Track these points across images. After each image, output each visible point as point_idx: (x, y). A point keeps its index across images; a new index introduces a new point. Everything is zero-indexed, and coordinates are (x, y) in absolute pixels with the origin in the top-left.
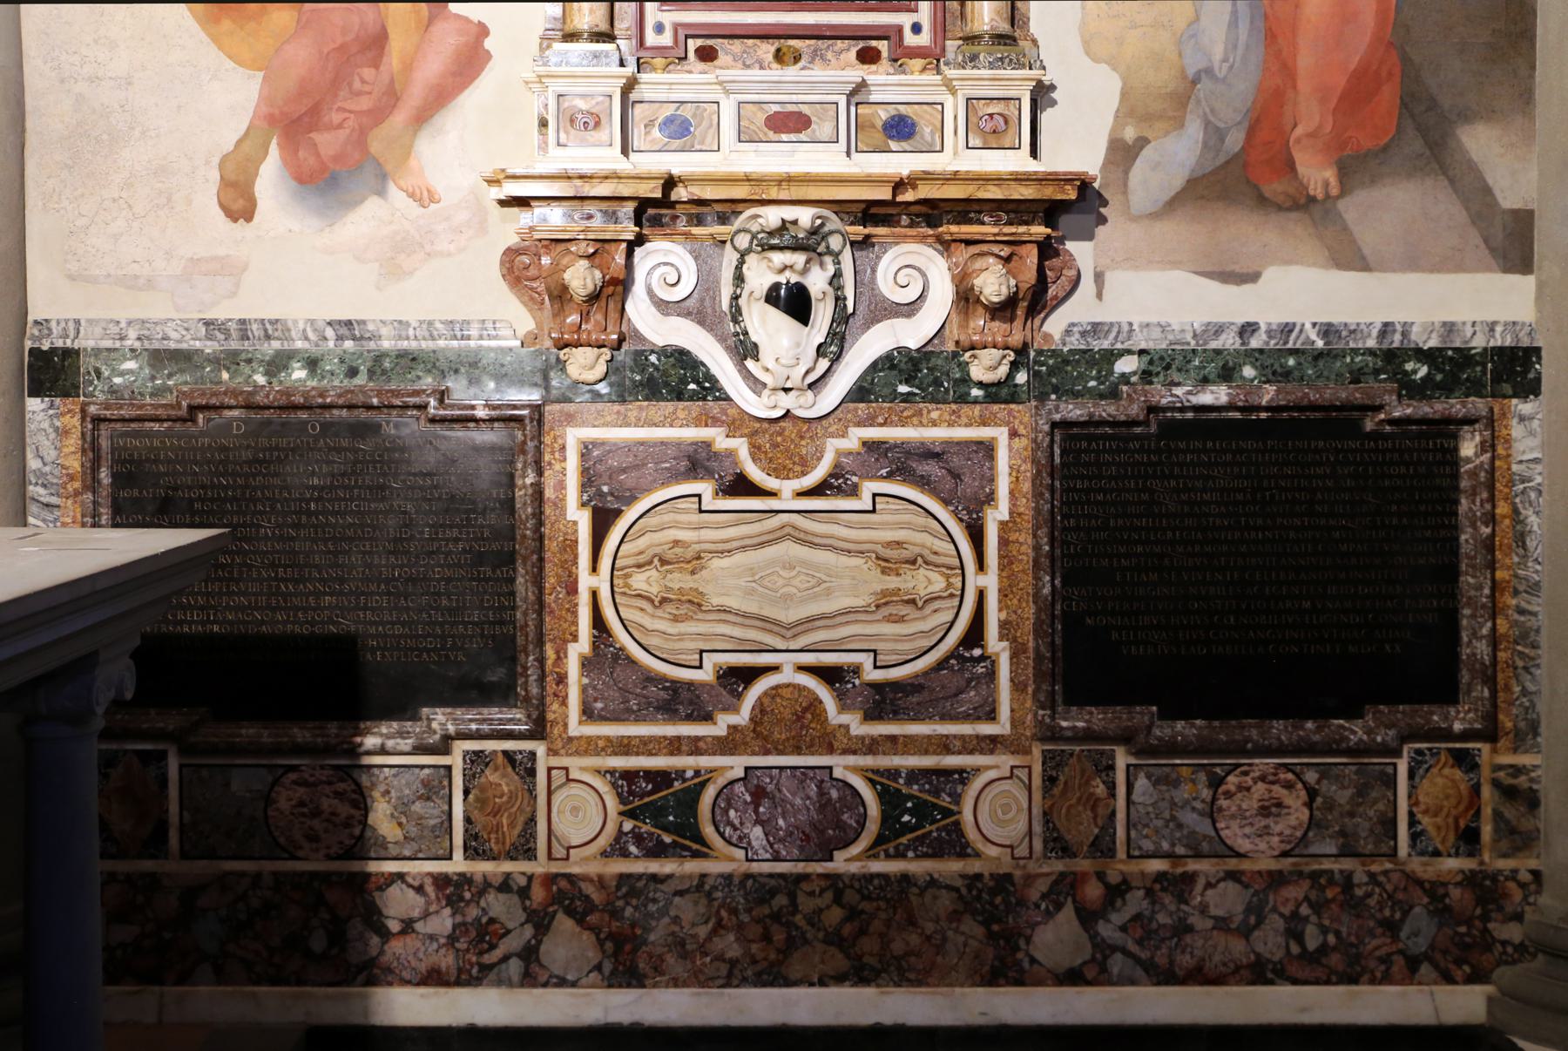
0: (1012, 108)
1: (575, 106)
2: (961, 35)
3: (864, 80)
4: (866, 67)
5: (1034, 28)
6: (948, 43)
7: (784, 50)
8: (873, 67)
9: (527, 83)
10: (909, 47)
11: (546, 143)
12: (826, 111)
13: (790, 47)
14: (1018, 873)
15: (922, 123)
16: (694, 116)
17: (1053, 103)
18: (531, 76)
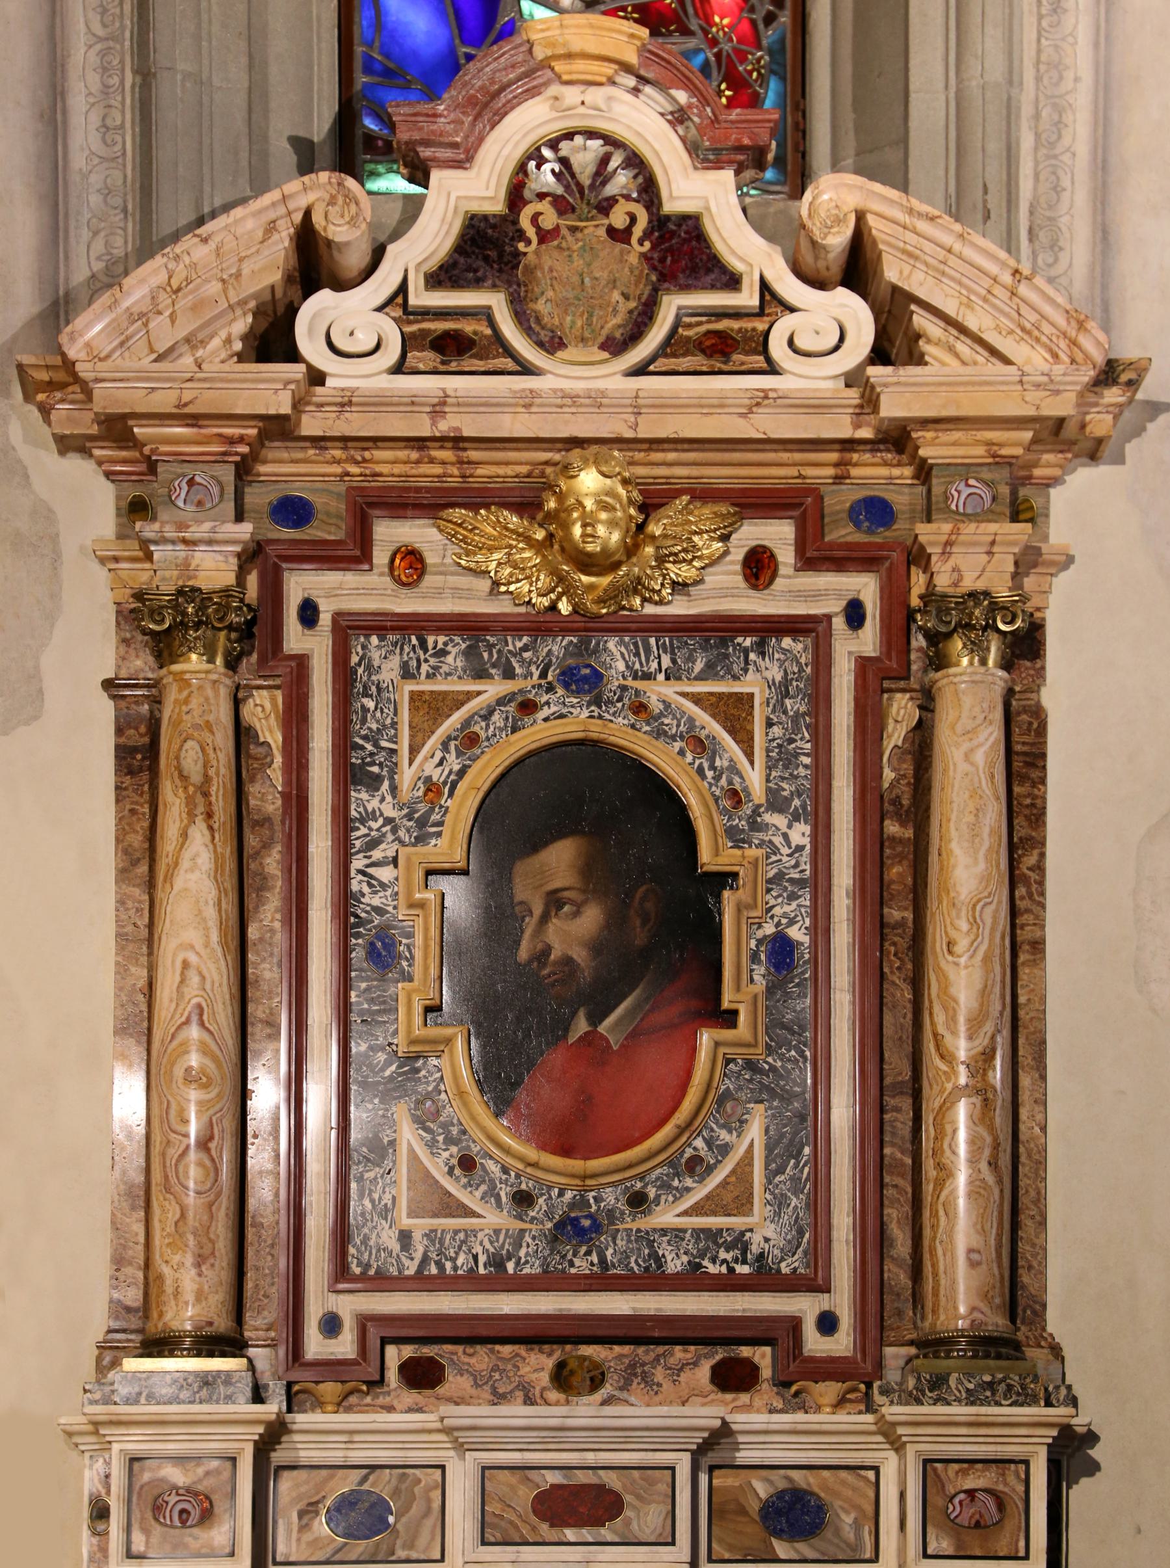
0: (1011, 1479)
1: (163, 1480)
2: (914, 1336)
3: (725, 1423)
4: (729, 1397)
5: (1054, 1323)
6: (889, 1351)
7: (573, 1364)
8: (744, 1398)
9: (70, 1434)
10: (812, 1359)
11: (104, 1550)
12: (652, 1483)
13: (584, 1358)
15: (837, 1503)
16: (396, 1493)
17: (1093, 1468)
18: (74, 1420)
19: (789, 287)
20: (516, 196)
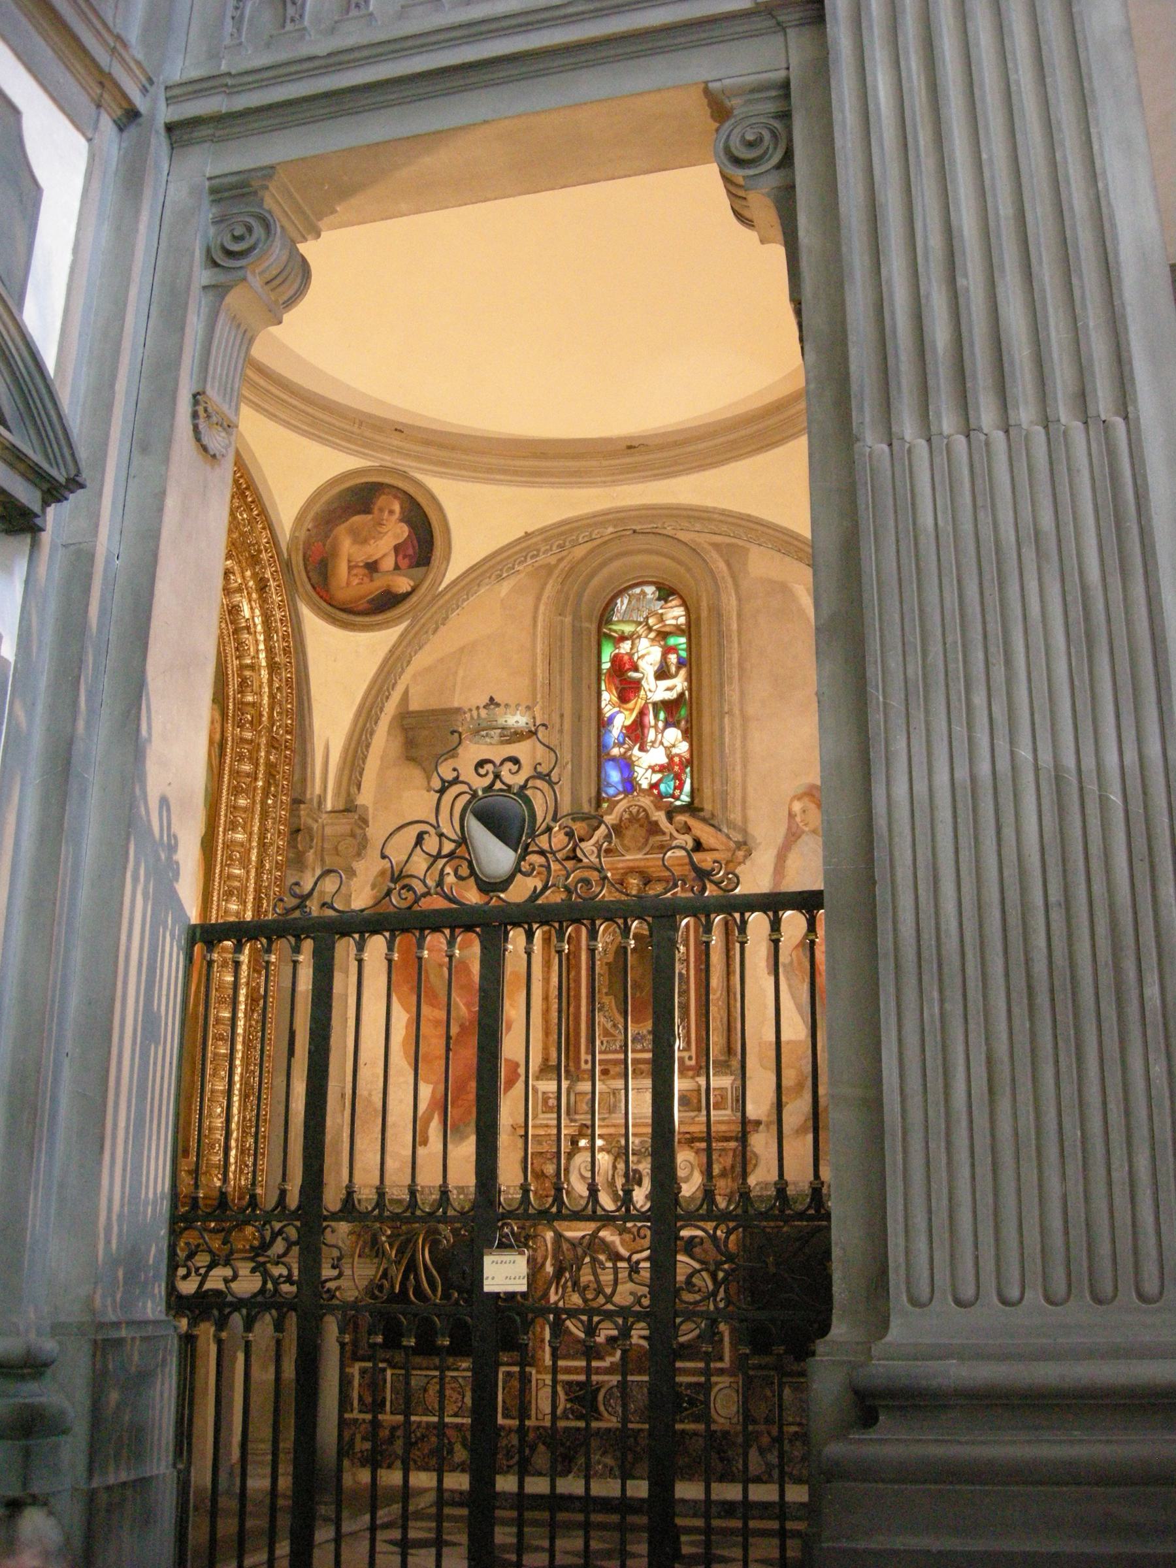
14: (732, 1432)
19: (675, 834)
20: (621, 820)
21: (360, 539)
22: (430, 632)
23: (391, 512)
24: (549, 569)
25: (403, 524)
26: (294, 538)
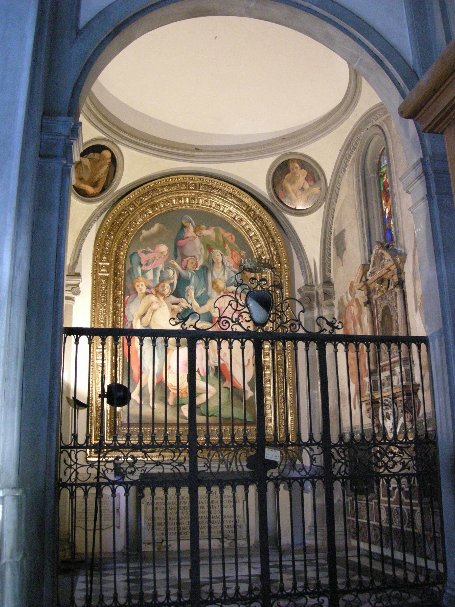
21: (292, 182)
22: (334, 202)
23: (296, 168)
24: (354, 159)
25: (303, 170)
26: (270, 194)
